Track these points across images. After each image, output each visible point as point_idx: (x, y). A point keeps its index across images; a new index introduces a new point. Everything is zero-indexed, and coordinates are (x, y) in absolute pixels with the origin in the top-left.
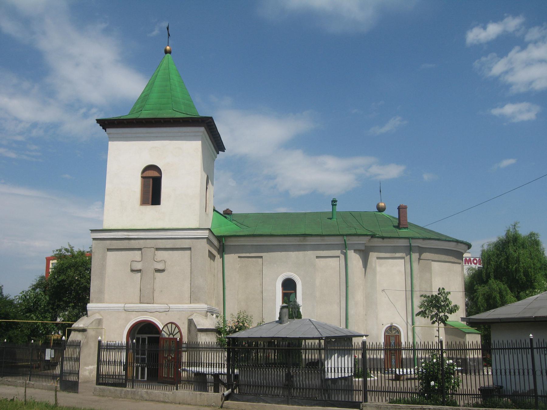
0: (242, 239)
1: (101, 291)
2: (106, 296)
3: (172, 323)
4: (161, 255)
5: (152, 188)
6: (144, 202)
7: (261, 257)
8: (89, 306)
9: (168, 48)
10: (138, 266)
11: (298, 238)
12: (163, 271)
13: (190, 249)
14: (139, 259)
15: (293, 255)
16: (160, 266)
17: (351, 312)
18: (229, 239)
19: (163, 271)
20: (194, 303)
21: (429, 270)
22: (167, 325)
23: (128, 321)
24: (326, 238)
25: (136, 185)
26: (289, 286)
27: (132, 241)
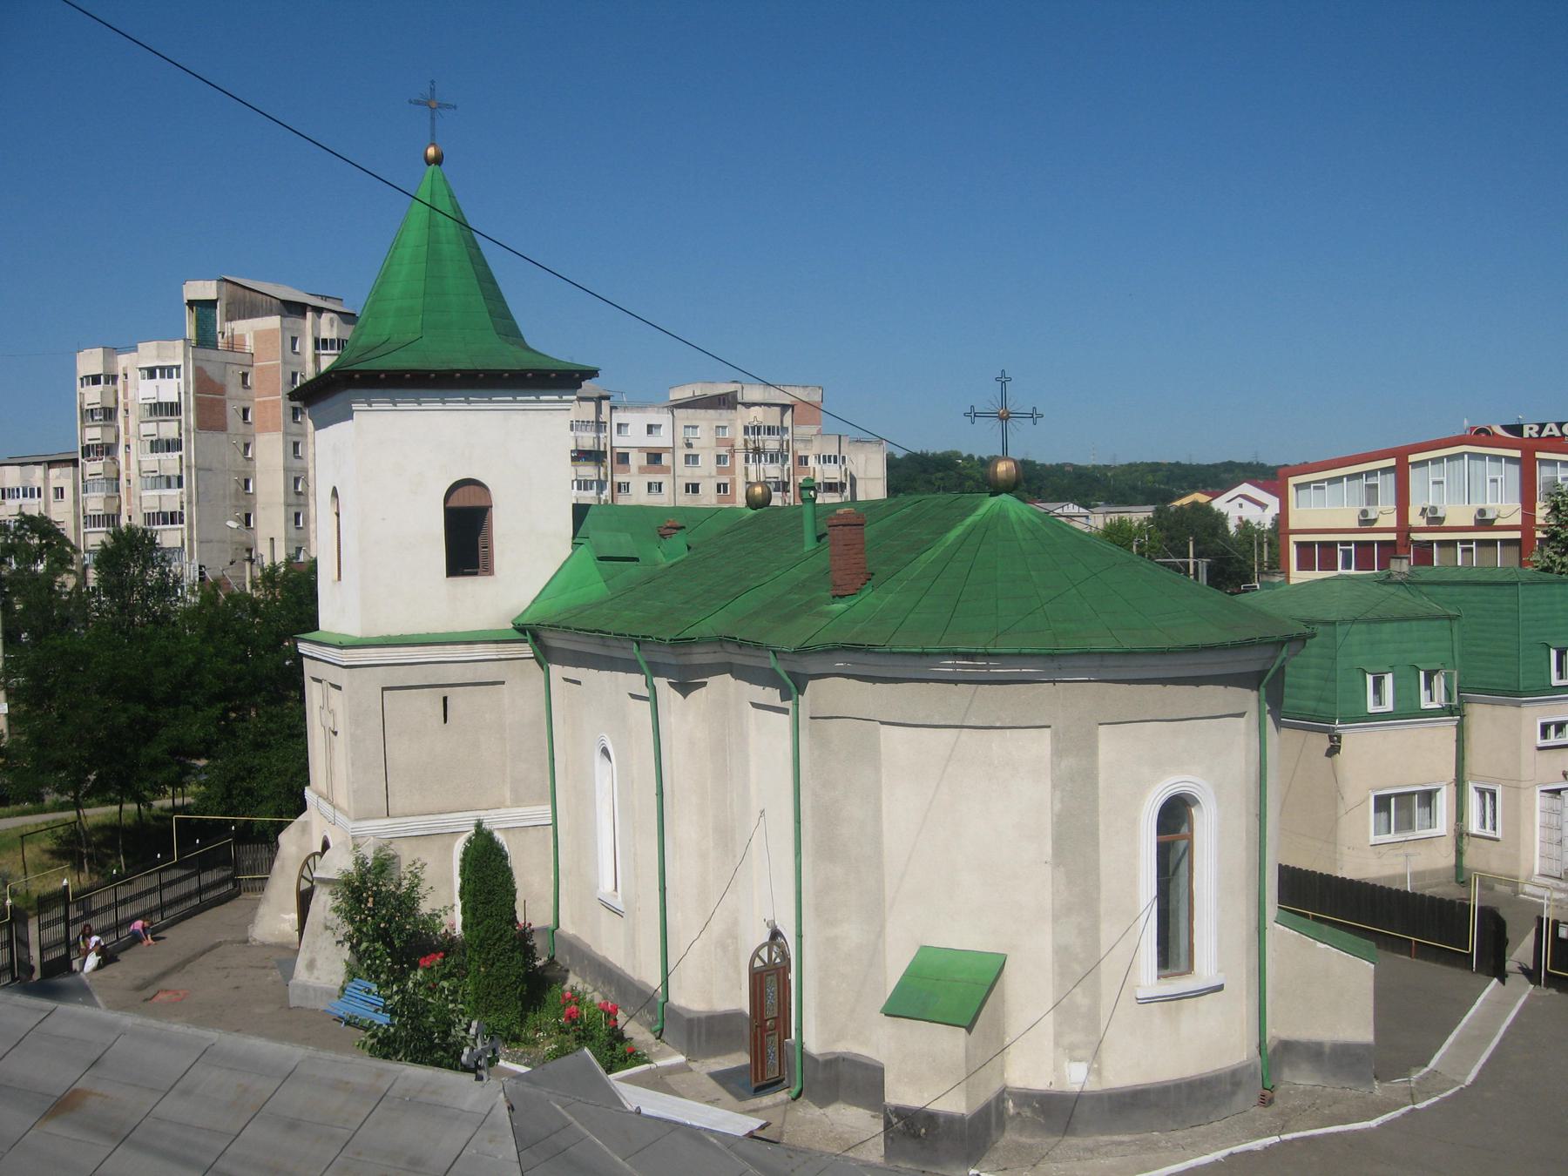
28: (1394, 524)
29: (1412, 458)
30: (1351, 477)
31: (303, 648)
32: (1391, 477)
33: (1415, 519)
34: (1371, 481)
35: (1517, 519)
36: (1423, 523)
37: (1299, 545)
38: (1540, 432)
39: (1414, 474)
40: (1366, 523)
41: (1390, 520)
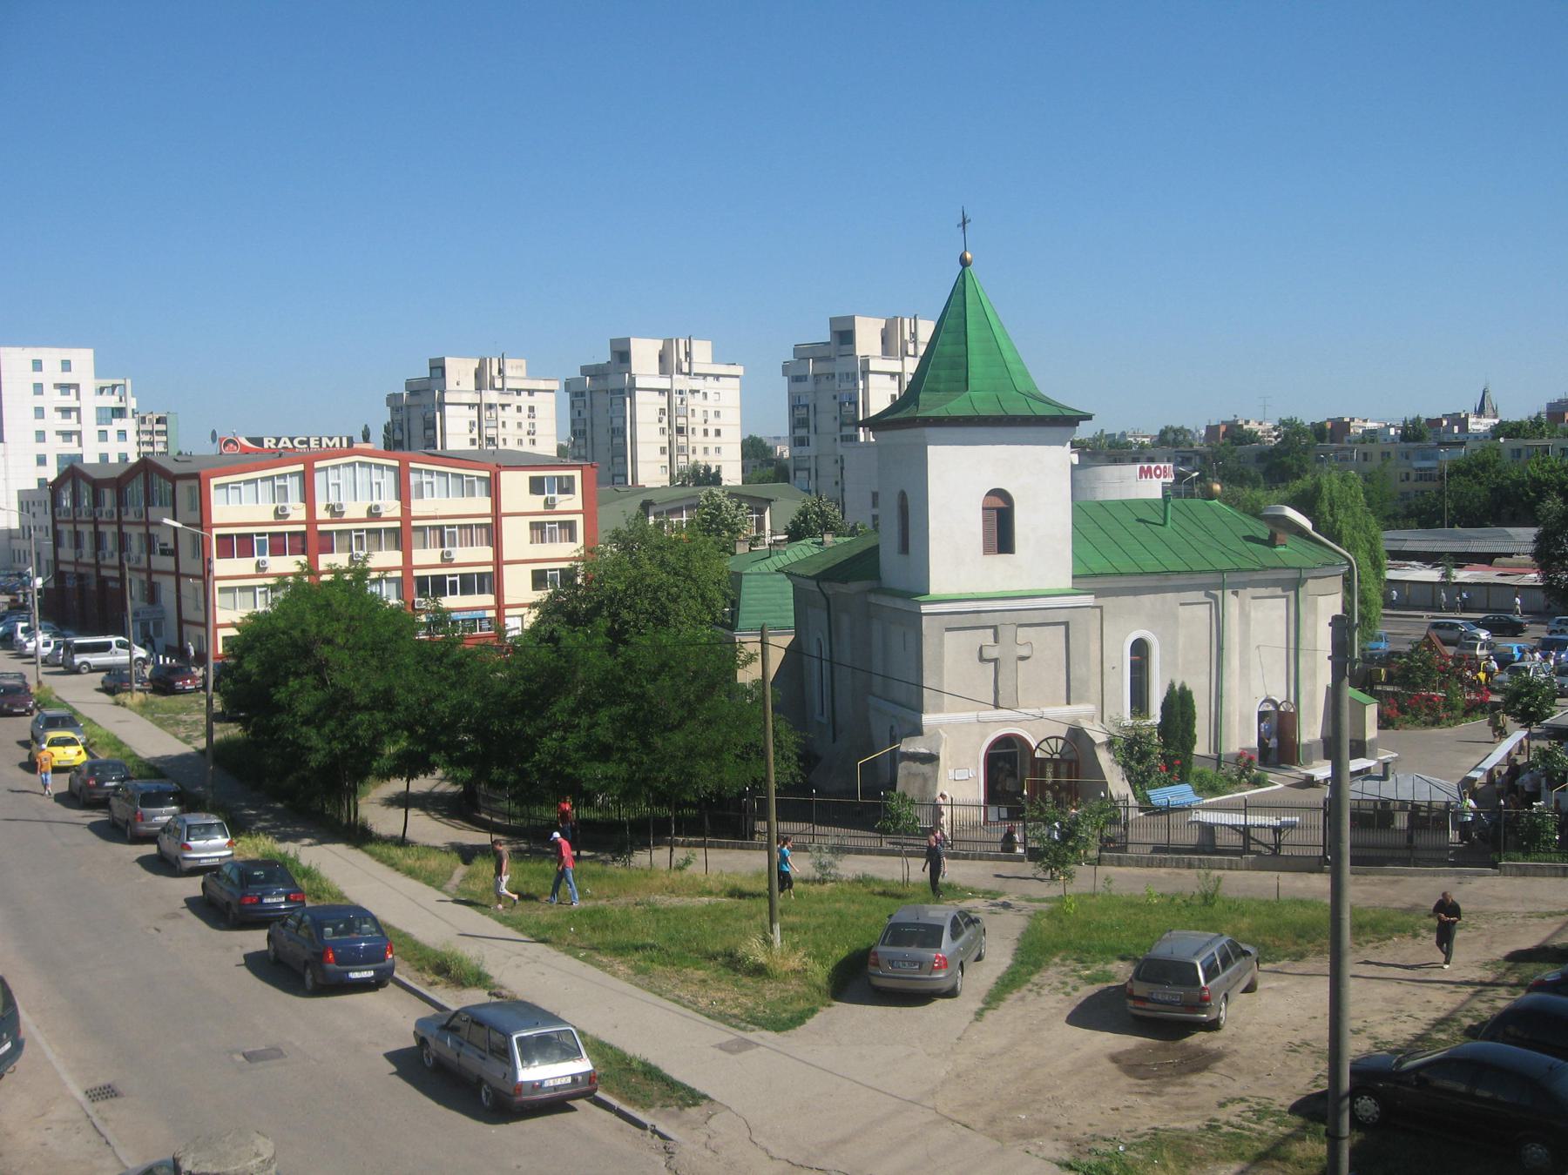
5: (1001, 528)
6: (987, 550)
7: (1101, 607)
8: (928, 719)
10: (990, 653)
13: (1066, 624)
15: (1147, 599)
16: (1024, 652)
23: (984, 737)
25: (973, 524)
26: (1140, 649)
29: (318, 465)
31: (925, 609)
32: (296, 480)
33: (322, 514)
34: (281, 482)
35: (398, 513)
36: (327, 516)
39: (319, 478)
40: (281, 515)
41: (302, 516)
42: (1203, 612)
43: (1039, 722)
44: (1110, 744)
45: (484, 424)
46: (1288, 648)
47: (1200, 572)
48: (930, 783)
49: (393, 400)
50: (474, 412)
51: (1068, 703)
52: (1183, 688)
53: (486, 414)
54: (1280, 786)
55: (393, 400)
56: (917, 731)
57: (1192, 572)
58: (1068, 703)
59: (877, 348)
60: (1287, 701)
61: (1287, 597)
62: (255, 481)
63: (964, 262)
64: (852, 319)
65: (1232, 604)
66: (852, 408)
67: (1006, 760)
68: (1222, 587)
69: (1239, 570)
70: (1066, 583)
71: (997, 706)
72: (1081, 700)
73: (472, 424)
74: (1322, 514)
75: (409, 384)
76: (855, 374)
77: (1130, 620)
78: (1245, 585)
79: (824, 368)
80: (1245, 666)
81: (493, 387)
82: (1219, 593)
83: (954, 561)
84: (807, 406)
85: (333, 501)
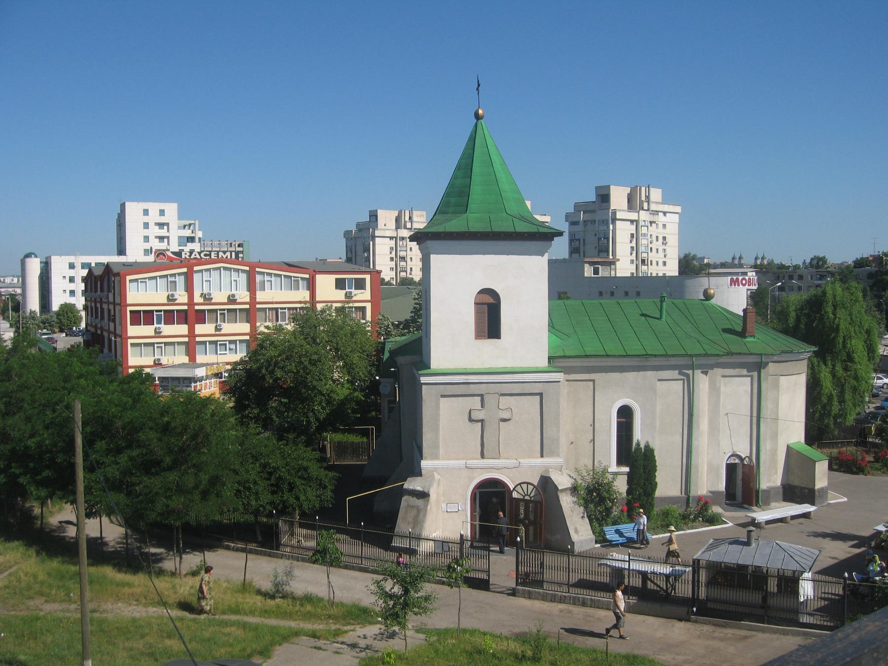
0: (570, 360)
1: (436, 446)
2: (441, 451)
3: (528, 483)
4: (505, 401)
5: (489, 317)
6: (479, 335)
7: (594, 381)
9: (480, 112)
11: (637, 359)
12: (509, 420)
13: (541, 395)
14: (479, 406)
15: (631, 375)
16: (505, 415)
17: (695, 443)
18: (557, 360)
19: (509, 420)
20: (547, 456)
21: (776, 386)
22: (520, 484)
23: (471, 480)
24: (671, 359)
26: (625, 413)
27: (472, 385)
28: (186, 301)
29: (196, 268)
30: (161, 277)
31: (423, 380)
32: (182, 278)
33: (198, 299)
35: (248, 299)
36: (201, 300)
37: (131, 311)
38: (190, 256)
39: (197, 278)
40: (171, 299)
42: (677, 387)
43: (517, 470)
44: (574, 490)
45: (399, 249)
46: (751, 416)
47: (673, 356)
48: (422, 514)
49: (347, 234)
50: (393, 242)
51: (542, 456)
52: (647, 446)
53: (400, 243)
54: (730, 524)
55: (347, 234)
56: (416, 472)
57: (666, 356)
58: (542, 456)
59: (625, 205)
60: (750, 458)
61: (752, 377)
62: (155, 278)
63: (478, 117)
64: (609, 187)
65: (702, 382)
66: (606, 241)
67: (490, 498)
68: (692, 367)
69: (706, 355)
70: (544, 363)
71: (483, 456)
72: (553, 454)
73: (391, 249)
74: (826, 312)
75: (358, 225)
76: (607, 221)
77: (616, 391)
78: (712, 367)
79: (589, 217)
80: (714, 429)
81: (405, 228)
82: (690, 372)
83: (452, 343)
84: (579, 240)
85: (205, 292)
